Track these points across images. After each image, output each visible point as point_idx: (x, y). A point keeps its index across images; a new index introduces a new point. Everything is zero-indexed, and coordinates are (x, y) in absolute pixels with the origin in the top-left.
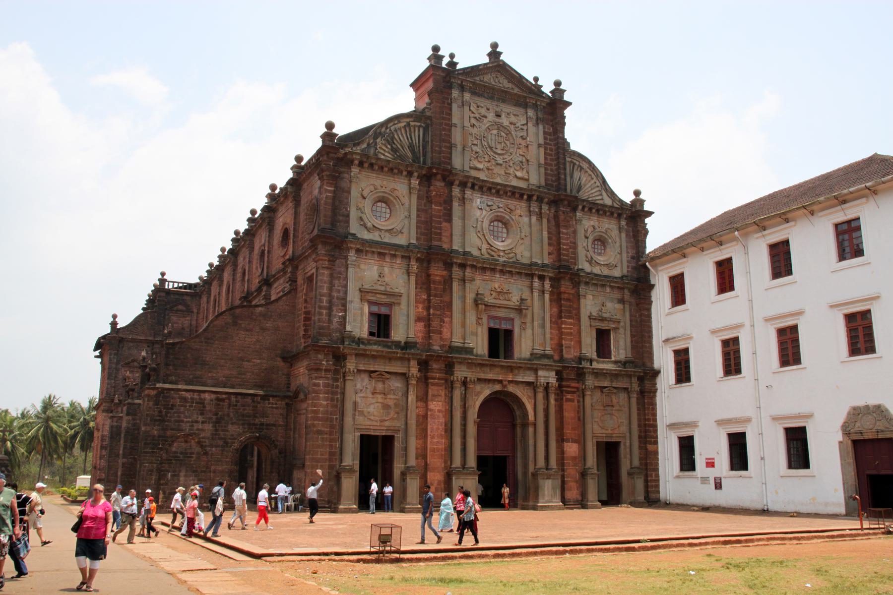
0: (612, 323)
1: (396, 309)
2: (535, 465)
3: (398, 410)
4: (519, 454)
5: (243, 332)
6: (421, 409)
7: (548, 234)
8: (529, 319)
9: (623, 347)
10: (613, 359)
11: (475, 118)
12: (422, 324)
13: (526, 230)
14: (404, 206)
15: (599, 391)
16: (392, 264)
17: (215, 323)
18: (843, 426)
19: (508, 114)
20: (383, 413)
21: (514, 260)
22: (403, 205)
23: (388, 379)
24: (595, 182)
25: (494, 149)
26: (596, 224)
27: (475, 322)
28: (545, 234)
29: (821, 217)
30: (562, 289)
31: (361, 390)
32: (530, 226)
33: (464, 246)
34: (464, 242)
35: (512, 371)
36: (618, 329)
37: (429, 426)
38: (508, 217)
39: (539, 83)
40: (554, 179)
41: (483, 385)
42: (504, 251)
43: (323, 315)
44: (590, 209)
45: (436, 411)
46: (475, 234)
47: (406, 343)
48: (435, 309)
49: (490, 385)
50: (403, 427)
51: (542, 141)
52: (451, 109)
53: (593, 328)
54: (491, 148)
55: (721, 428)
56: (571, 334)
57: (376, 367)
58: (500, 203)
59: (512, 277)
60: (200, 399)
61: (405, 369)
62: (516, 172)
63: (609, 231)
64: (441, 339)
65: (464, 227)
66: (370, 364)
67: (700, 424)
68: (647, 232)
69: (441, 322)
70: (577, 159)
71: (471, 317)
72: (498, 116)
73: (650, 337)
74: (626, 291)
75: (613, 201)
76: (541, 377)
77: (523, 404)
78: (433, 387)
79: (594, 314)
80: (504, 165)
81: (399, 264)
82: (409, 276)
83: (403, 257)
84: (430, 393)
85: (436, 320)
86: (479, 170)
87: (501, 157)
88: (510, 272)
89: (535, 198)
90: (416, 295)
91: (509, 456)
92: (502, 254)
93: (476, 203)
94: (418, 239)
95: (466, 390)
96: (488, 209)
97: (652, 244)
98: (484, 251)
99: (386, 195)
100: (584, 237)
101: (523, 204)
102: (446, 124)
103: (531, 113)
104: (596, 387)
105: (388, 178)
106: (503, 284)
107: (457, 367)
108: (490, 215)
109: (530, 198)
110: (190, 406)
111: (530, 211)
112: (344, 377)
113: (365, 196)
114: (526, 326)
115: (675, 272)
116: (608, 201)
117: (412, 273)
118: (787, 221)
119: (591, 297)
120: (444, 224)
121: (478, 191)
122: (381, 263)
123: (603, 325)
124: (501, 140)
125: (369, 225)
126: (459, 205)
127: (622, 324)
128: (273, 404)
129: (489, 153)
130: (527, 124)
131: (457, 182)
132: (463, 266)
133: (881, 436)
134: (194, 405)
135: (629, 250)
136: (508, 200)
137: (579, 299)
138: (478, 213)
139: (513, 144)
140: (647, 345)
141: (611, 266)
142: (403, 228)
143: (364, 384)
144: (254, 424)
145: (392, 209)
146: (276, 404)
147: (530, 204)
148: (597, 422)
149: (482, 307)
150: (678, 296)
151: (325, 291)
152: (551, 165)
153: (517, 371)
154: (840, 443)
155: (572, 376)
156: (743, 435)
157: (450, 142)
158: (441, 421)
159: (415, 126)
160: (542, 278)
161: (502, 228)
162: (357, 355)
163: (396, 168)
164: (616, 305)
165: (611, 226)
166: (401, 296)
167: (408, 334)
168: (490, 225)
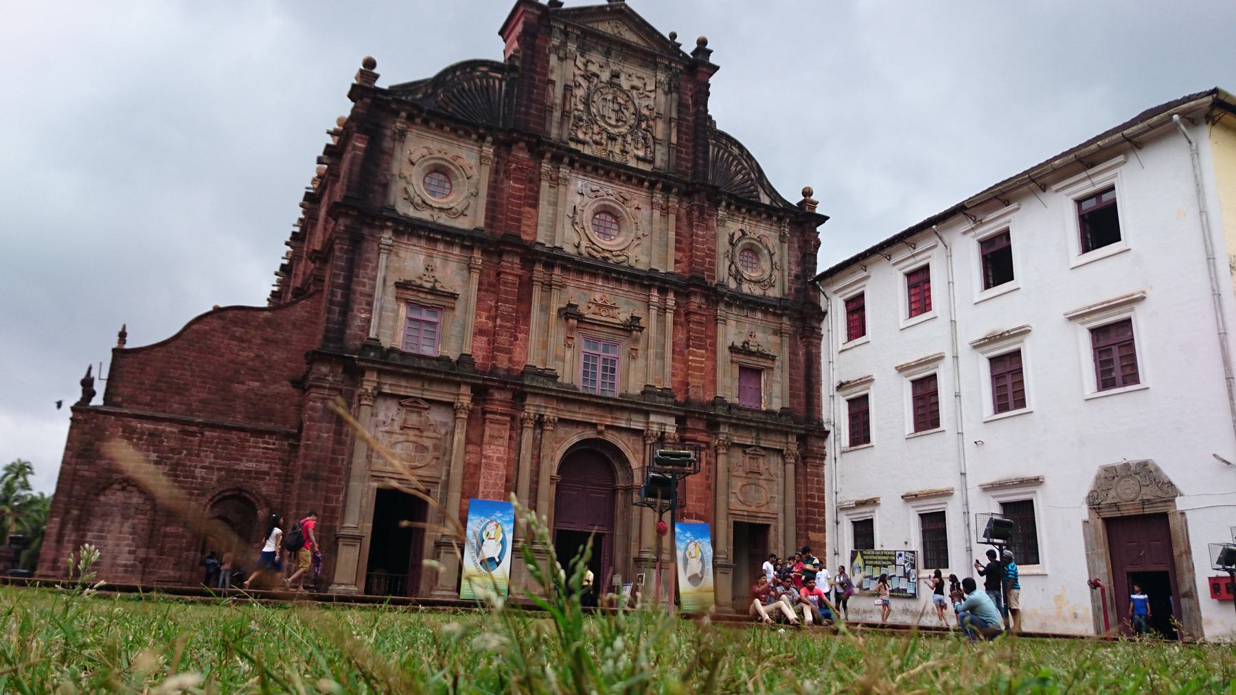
0: (764, 360)
1: (448, 313)
2: (640, 548)
3: (437, 453)
4: (619, 532)
5: (235, 343)
6: (474, 456)
7: (676, 235)
8: (641, 346)
9: (780, 394)
10: (763, 408)
11: (582, 76)
12: (485, 339)
13: (644, 227)
14: (471, 180)
15: (741, 451)
16: (445, 254)
17: (195, 327)
18: (1089, 496)
19: (630, 76)
20: (415, 457)
21: (625, 264)
22: (468, 178)
23: (426, 409)
24: (749, 175)
25: (607, 119)
26: (747, 229)
27: (563, 342)
28: (672, 234)
29: (1057, 191)
30: (693, 307)
31: (384, 423)
32: (651, 223)
33: (553, 238)
34: (554, 236)
35: (611, 412)
36: (772, 369)
37: (482, 481)
38: (620, 209)
39: (677, 40)
40: (689, 165)
41: (567, 429)
42: (611, 251)
43: (334, 314)
44: (738, 209)
45: (495, 458)
46: (570, 226)
47: (458, 362)
48: (503, 318)
49: (579, 430)
50: (443, 478)
51: (674, 115)
52: (548, 62)
53: (734, 365)
54: (603, 117)
55: (909, 505)
56: (702, 368)
57: (409, 390)
58: (610, 190)
59: (621, 286)
60: (156, 430)
61: (453, 397)
63: (764, 239)
64: (510, 360)
65: (555, 215)
66: (401, 386)
67: (881, 501)
68: (818, 244)
69: (511, 337)
70: (724, 142)
71: (558, 334)
72: (616, 75)
73: (819, 383)
74: (785, 320)
75: (772, 200)
76: (653, 423)
77: (627, 460)
78: (492, 425)
79: (739, 344)
80: (620, 140)
81: (455, 255)
82: (470, 273)
83: (463, 247)
84: (487, 432)
85: (505, 334)
86: (584, 143)
87: (616, 131)
88: (618, 281)
89: (659, 186)
90: (479, 300)
91: (604, 534)
92: (607, 255)
93: (576, 185)
94: (486, 224)
95: (541, 433)
96: (593, 195)
97: (825, 261)
98: (583, 250)
99: (446, 164)
100: (728, 244)
101: (642, 193)
102: (540, 81)
103: (662, 77)
104: (734, 445)
105: (450, 141)
106: (607, 295)
107: (529, 400)
108: (594, 203)
109: (652, 186)
110: (140, 439)
111: (652, 203)
112: (360, 401)
113: (414, 161)
114: (637, 354)
115: (852, 292)
116: (765, 200)
117: (474, 268)
118: (1007, 203)
119: (733, 323)
120: (527, 209)
121: (577, 169)
122: (430, 251)
123: (749, 361)
124: (616, 107)
125: (417, 200)
126: (550, 186)
127: (777, 363)
128: (268, 443)
129: (599, 123)
130: (655, 91)
131: (548, 155)
132: (549, 266)
133: (1148, 511)
134: (145, 437)
135: (793, 267)
137: (717, 324)
138: (579, 196)
139: (633, 114)
140: (816, 394)
141: (765, 286)
142: (466, 208)
143: (390, 415)
144: (236, 470)
145: (453, 182)
146: (274, 444)
147: (652, 193)
148: (735, 493)
149: (573, 322)
150: (856, 328)
151: (341, 281)
152: (686, 147)
153: (618, 415)
154: (1086, 522)
155: (701, 426)
156: (941, 516)
157: (543, 104)
158: (500, 473)
159: (494, 78)
160: (663, 291)
161: (612, 223)
162: (381, 372)
163: (462, 129)
164: (769, 338)
165: (767, 233)
166: (456, 299)
167: (461, 348)
168: (594, 218)
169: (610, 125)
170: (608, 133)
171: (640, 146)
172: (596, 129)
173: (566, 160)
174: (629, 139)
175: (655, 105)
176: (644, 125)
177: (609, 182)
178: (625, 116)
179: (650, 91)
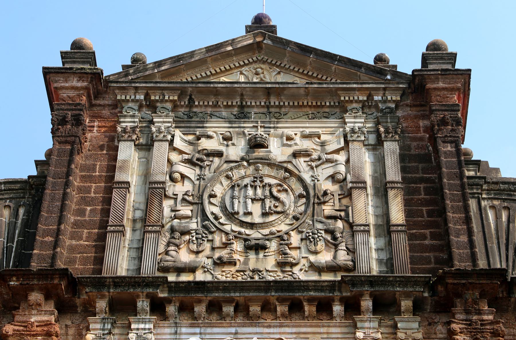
54: (232, 216)
62: (312, 258)
80: (273, 245)
86: (192, 270)
87: (266, 231)
89: (367, 303)
129: (227, 228)
136: (281, 326)
139: (301, 196)
169: (252, 226)
170: (246, 240)
171: (321, 245)
172: (218, 239)
173: (143, 304)
174: (295, 239)
175: (348, 171)
176: (328, 209)
177: (251, 326)
178: (283, 203)
179: (337, 151)
